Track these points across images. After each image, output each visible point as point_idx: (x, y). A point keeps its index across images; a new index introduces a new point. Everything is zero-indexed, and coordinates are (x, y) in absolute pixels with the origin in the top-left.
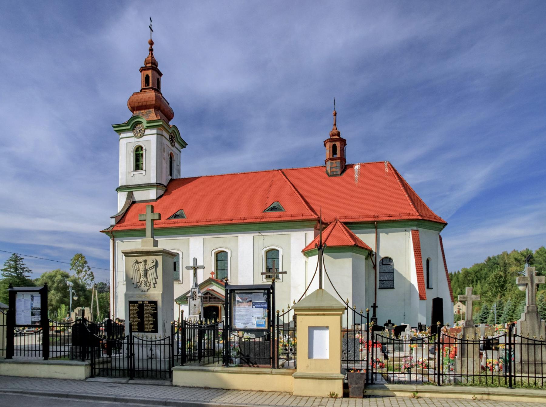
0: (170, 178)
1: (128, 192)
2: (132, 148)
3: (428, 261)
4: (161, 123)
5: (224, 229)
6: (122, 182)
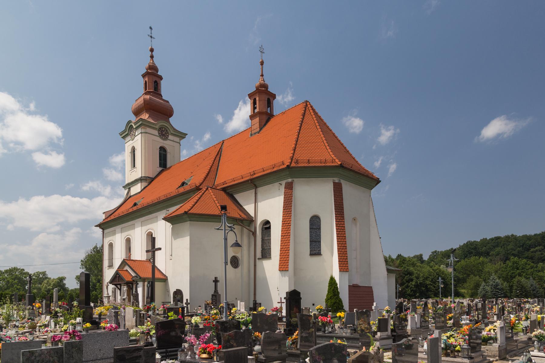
5: (148, 211)
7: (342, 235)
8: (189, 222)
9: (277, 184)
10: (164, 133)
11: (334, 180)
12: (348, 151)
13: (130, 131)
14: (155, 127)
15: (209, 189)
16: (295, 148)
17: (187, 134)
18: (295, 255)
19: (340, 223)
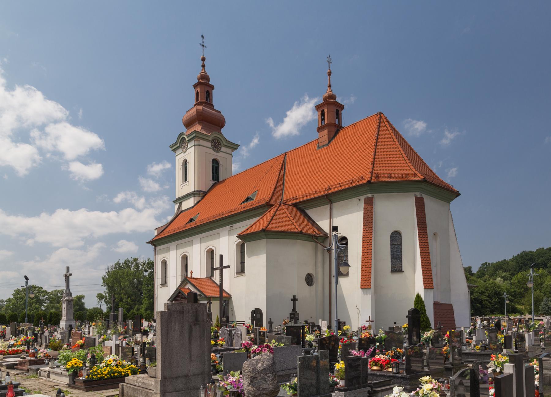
5: (209, 227)
7: (426, 251)
8: (265, 239)
9: (355, 200)
10: (217, 144)
11: (415, 195)
12: (425, 164)
13: (181, 143)
14: (208, 138)
15: (282, 205)
16: (374, 162)
17: (239, 145)
18: (375, 272)
19: (423, 239)
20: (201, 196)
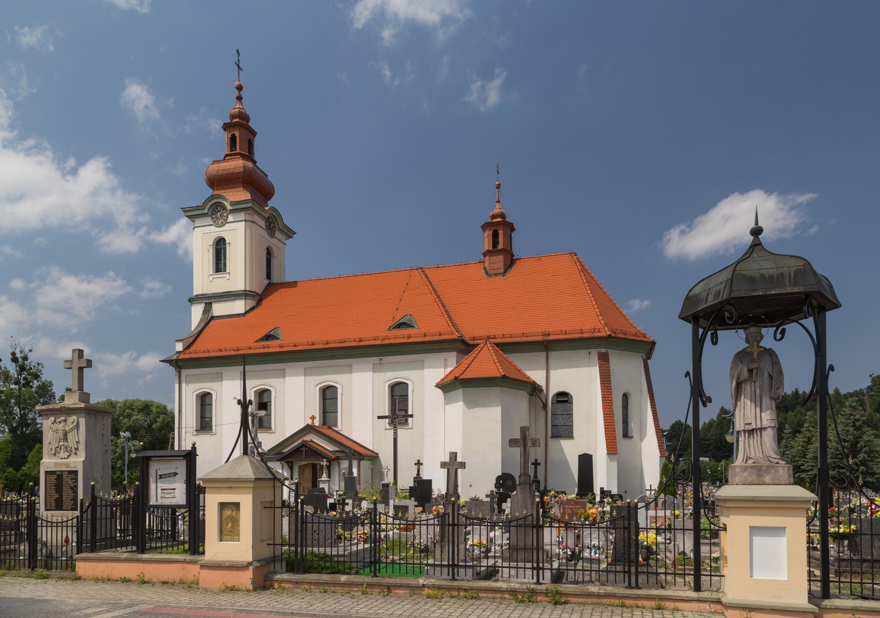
0: (267, 282)
1: (206, 304)
2: (211, 241)
3: (625, 397)
4: (250, 205)
6: (197, 290)
20: (256, 299)
